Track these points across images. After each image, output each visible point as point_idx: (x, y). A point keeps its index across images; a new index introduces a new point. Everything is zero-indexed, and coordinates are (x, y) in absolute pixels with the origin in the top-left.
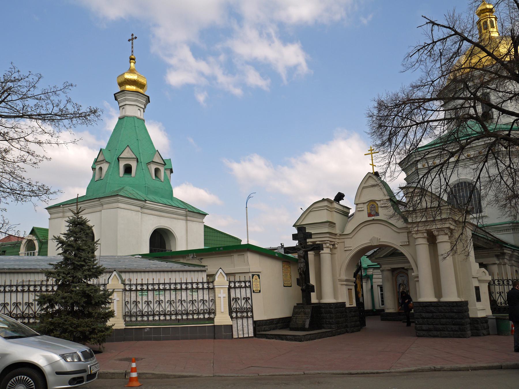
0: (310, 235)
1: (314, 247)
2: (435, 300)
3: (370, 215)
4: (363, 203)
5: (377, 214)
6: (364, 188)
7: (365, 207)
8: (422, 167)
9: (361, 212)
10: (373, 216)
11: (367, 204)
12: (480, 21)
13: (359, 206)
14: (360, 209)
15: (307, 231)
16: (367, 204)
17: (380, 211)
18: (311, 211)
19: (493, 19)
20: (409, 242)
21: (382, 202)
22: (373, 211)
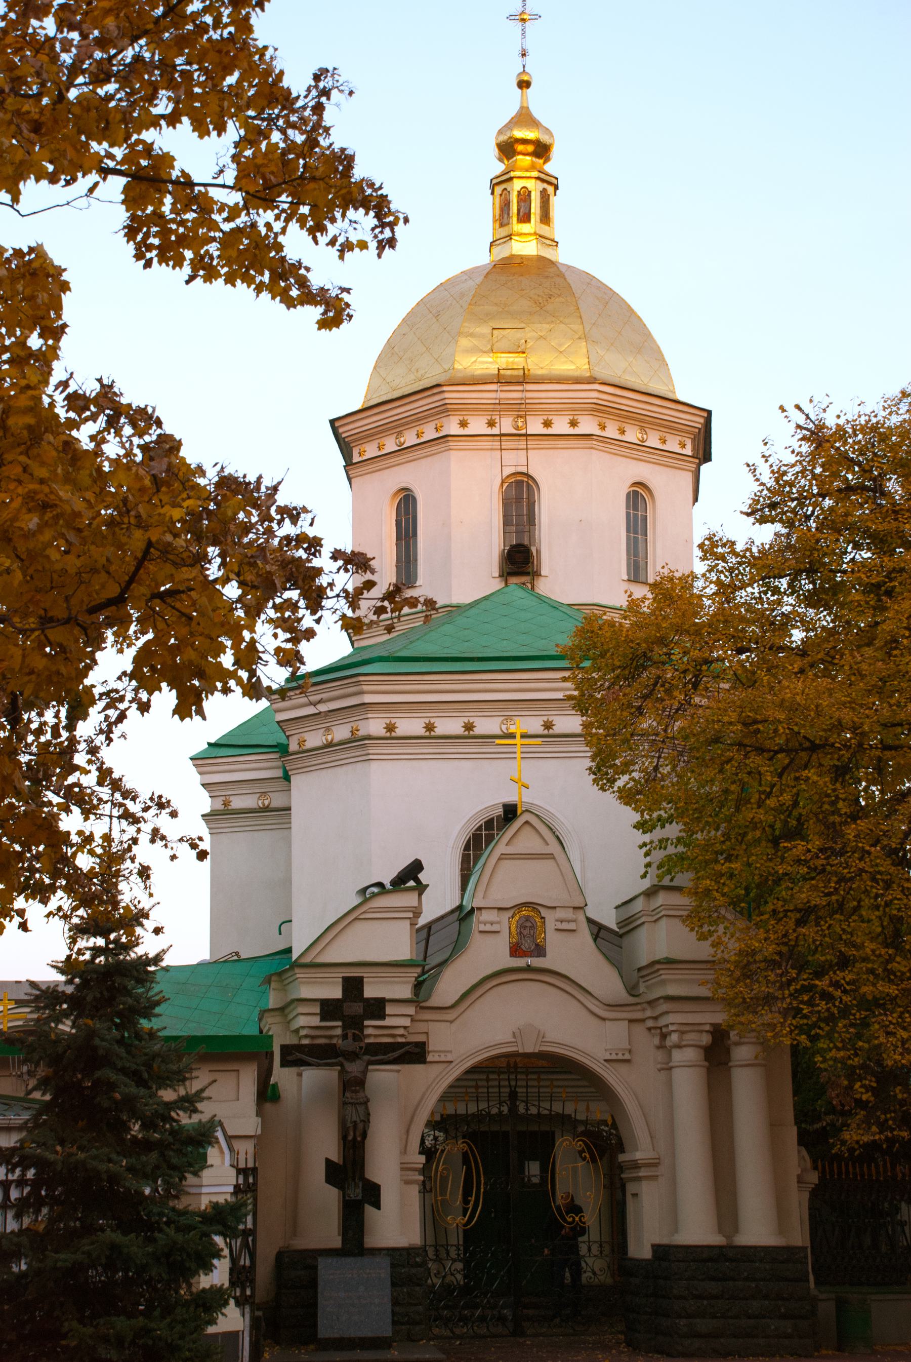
0: (378, 1008)
1: (407, 1052)
2: (716, 1240)
3: (516, 951)
4: (500, 909)
5: (540, 951)
6: (503, 857)
7: (504, 924)
8: (382, 732)
9: (490, 939)
10: (524, 954)
11: (510, 913)
12: (511, 179)
13: (485, 916)
14: (488, 928)
15: (370, 991)
16: (510, 913)
17: (552, 940)
18: (356, 919)
19: (550, 189)
20: (630, 1051)
21: (560, 914)
22: (527, 940)
